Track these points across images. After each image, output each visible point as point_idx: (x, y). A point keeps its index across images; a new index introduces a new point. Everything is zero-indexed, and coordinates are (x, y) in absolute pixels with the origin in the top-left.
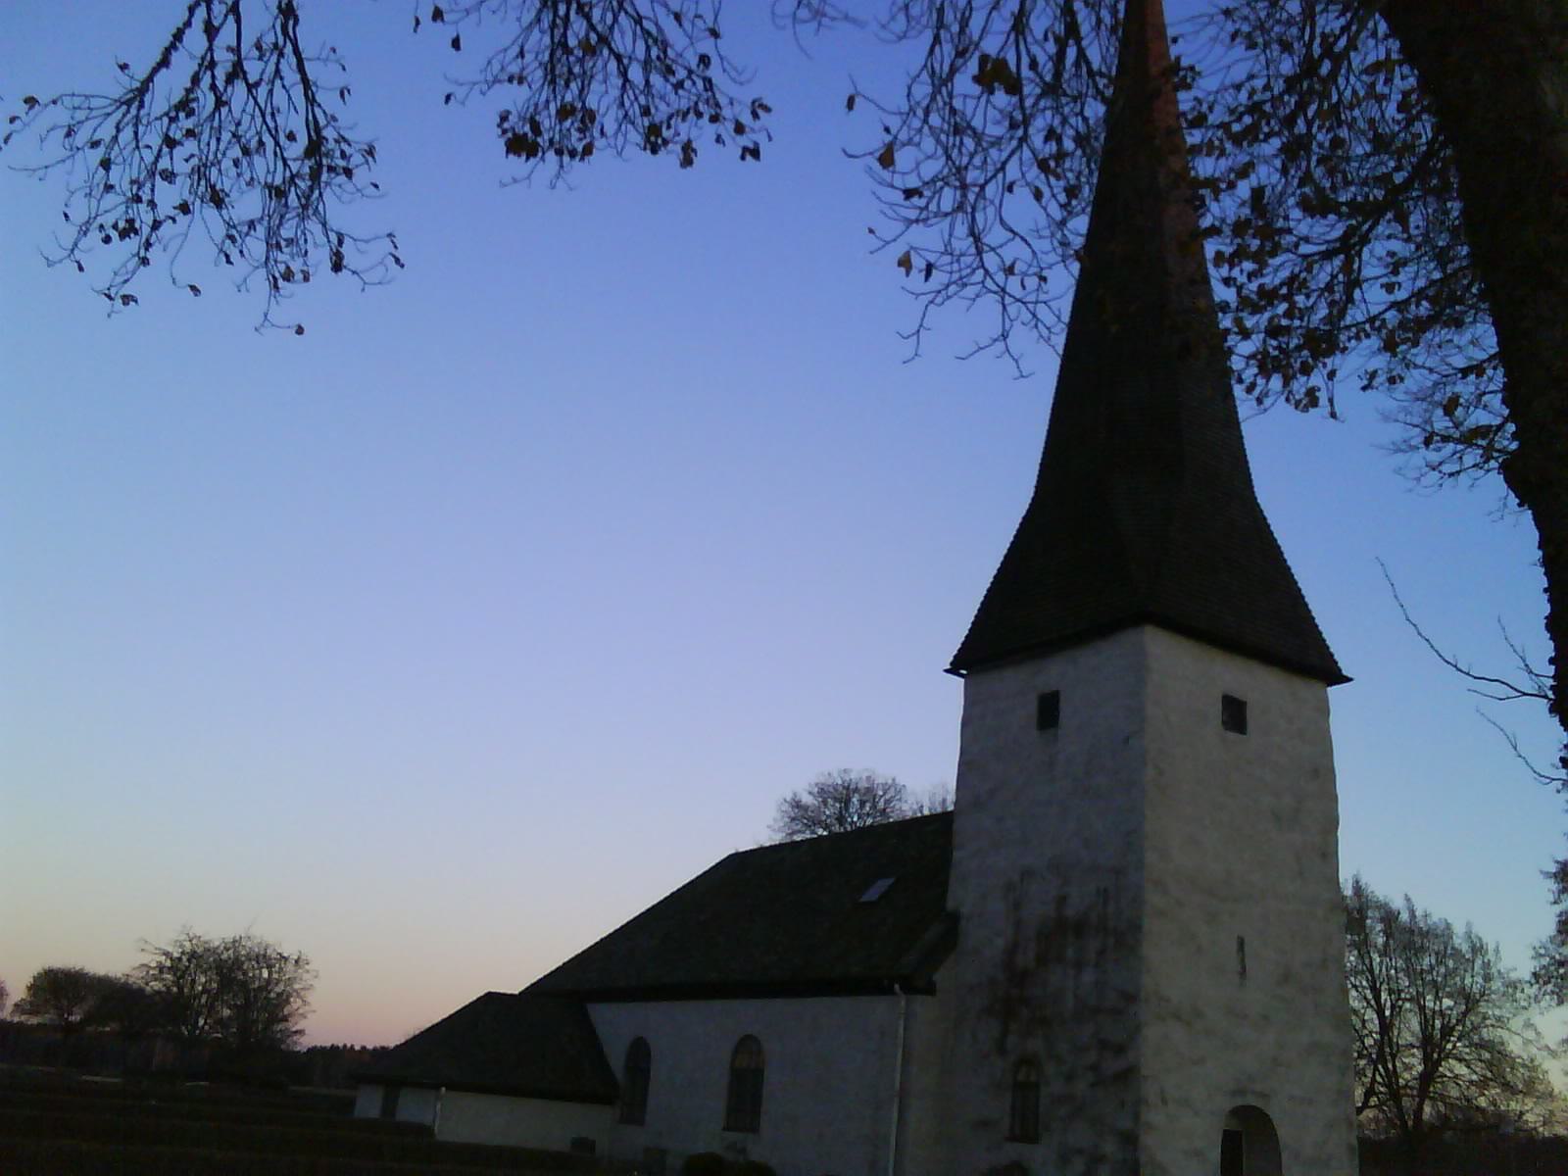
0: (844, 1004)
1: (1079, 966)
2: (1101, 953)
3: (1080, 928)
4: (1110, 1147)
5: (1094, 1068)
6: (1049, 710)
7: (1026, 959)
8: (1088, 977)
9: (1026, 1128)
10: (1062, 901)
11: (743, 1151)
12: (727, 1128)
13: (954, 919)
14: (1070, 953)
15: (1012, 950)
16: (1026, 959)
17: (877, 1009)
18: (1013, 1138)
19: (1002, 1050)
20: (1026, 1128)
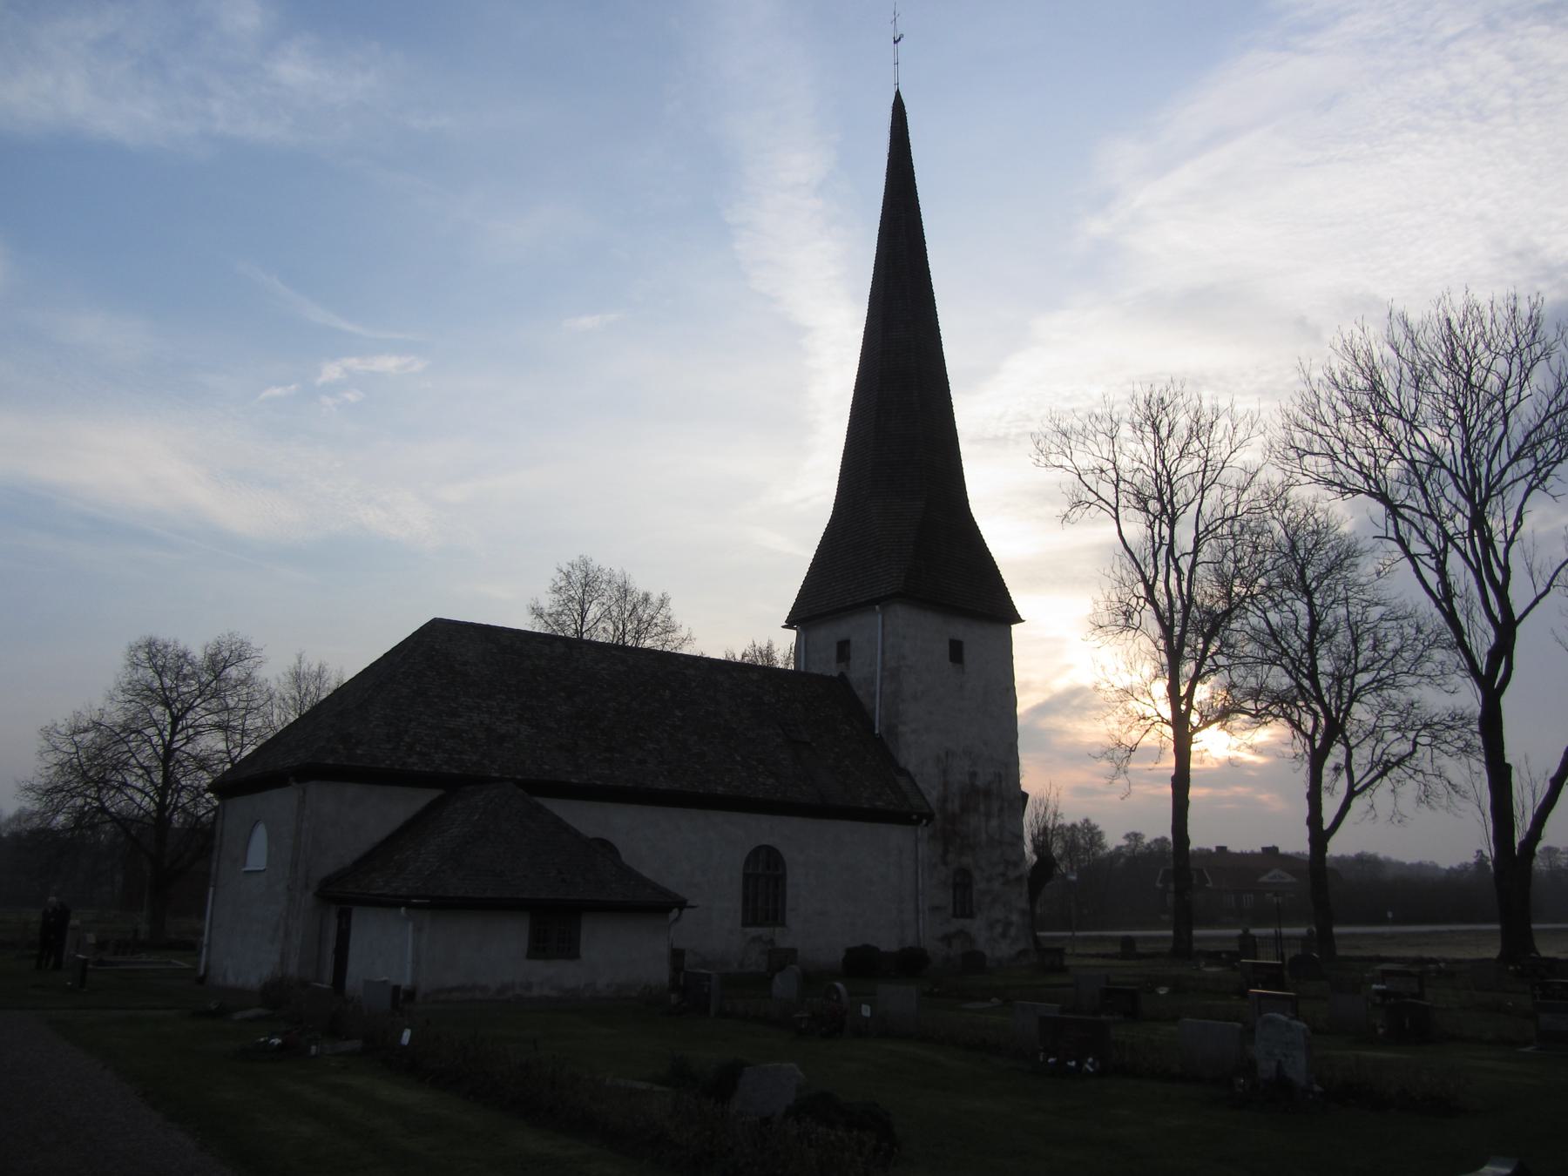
0: (866, 827)
1: (988, 815)
2: (1001, 810)
3: (987, 793)
4: (1015, 917)
5: (1003, 875)
6: (956, 651)
7: (954, 806)
8: (994, 823)
9: (964, 906)
10: (973, 775)
11: (772, 941)
12: (745, 924)
13: (904, 772)
14: (982, 808)
15: (944, 800)
16: (954, 806)
17: (896, 835)
18: (955, 916)
19: (945, 863)
20: (964, 906)
